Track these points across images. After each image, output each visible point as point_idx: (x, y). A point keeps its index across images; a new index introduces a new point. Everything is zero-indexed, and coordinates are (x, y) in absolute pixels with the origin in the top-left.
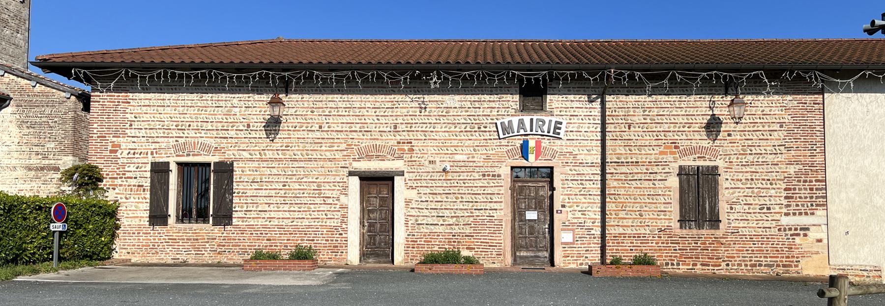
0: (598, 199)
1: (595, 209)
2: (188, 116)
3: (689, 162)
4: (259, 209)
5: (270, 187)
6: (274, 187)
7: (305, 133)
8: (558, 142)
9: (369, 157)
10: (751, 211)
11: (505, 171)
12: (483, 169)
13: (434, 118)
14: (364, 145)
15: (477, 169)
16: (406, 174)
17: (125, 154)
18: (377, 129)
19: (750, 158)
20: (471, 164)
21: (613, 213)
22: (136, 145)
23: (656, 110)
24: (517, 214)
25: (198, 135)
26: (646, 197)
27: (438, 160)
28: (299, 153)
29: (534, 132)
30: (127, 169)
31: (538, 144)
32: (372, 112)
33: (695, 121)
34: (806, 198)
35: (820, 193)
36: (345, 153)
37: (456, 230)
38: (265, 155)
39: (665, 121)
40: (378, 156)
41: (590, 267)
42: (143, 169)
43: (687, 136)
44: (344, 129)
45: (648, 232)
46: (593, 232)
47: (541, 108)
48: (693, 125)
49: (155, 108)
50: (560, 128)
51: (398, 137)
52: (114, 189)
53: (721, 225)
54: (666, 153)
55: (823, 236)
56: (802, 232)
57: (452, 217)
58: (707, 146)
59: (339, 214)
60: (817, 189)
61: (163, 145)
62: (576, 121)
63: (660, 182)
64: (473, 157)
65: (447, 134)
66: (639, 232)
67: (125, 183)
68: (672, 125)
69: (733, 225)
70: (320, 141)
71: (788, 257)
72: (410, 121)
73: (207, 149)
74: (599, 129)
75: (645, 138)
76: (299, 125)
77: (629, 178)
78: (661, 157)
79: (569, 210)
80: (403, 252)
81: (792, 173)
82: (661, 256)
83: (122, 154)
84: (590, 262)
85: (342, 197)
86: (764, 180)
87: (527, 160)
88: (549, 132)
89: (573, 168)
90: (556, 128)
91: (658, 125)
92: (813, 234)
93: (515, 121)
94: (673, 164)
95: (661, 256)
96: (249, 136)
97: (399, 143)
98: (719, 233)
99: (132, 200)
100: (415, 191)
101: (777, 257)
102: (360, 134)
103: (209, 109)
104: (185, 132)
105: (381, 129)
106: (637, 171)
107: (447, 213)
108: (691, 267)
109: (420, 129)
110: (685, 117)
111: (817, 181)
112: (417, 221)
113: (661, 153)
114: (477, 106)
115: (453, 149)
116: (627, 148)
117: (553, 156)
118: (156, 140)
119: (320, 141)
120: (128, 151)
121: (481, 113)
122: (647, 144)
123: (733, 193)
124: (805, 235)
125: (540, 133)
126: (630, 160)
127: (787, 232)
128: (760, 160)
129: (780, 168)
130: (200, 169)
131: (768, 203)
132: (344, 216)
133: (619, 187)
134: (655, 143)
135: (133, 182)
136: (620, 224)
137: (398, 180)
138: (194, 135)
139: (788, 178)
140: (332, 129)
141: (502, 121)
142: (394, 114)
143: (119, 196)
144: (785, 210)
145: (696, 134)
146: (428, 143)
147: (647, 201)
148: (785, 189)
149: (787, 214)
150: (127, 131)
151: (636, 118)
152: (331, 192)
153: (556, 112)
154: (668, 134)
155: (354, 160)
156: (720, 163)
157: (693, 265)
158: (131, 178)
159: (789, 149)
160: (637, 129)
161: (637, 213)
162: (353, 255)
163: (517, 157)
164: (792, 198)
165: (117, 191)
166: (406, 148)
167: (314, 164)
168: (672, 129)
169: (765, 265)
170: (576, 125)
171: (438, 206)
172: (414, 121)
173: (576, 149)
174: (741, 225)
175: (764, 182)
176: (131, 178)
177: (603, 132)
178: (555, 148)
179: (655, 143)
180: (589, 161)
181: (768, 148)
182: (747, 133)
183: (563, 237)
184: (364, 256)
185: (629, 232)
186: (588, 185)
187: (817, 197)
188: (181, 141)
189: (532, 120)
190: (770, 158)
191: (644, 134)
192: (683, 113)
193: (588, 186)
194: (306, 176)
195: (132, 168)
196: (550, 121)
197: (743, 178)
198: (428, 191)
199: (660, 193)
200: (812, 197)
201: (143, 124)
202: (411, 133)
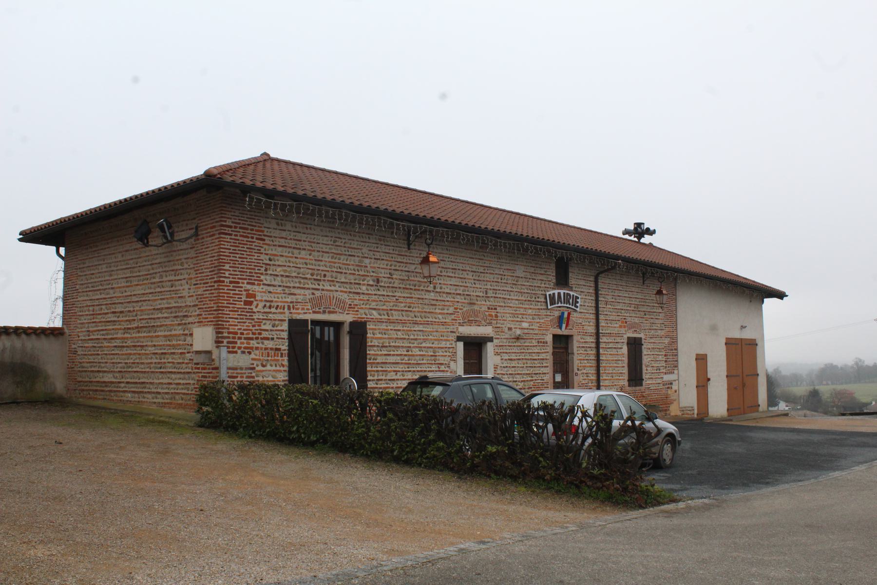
0: (594, 363)
4: (388, 378)
5: (396, 353)
6: (399, 353)
9: (470, 323)
11: (549, 338)
20: (531, 332)
22: (272, 295)
25: (333, 288)
30: (263, 327)
36: (453, 317)
38: (392, 315)
42: (279, 328)
49: (291, 250)
52: (250, 353)
67: (260, 345)
70: (434, 302)
73: (342, 306)
83: (258, 307)
85: (452, 363)
87: (561, 328)
92: (675, 387)
98: (642, 388)
99: (268, 367)
100: (499, 357)
103: (342, 257)
104: (321, 283)
118: (293, 291)
119: (434, 302)
120: (263, 303)
130: (326, 329)
135: (270, 344)
137: (490, 347)
138: (329, 288)
140: (443, 290)
143: (255, 363)
150: (262, 277)
155: (461, 325)
158: (267, 339)
165: (252, 356)
176: (267, 339)
188: (318, 294)
194: (425, 340)
195: (268, 327)
201: (279, 269)
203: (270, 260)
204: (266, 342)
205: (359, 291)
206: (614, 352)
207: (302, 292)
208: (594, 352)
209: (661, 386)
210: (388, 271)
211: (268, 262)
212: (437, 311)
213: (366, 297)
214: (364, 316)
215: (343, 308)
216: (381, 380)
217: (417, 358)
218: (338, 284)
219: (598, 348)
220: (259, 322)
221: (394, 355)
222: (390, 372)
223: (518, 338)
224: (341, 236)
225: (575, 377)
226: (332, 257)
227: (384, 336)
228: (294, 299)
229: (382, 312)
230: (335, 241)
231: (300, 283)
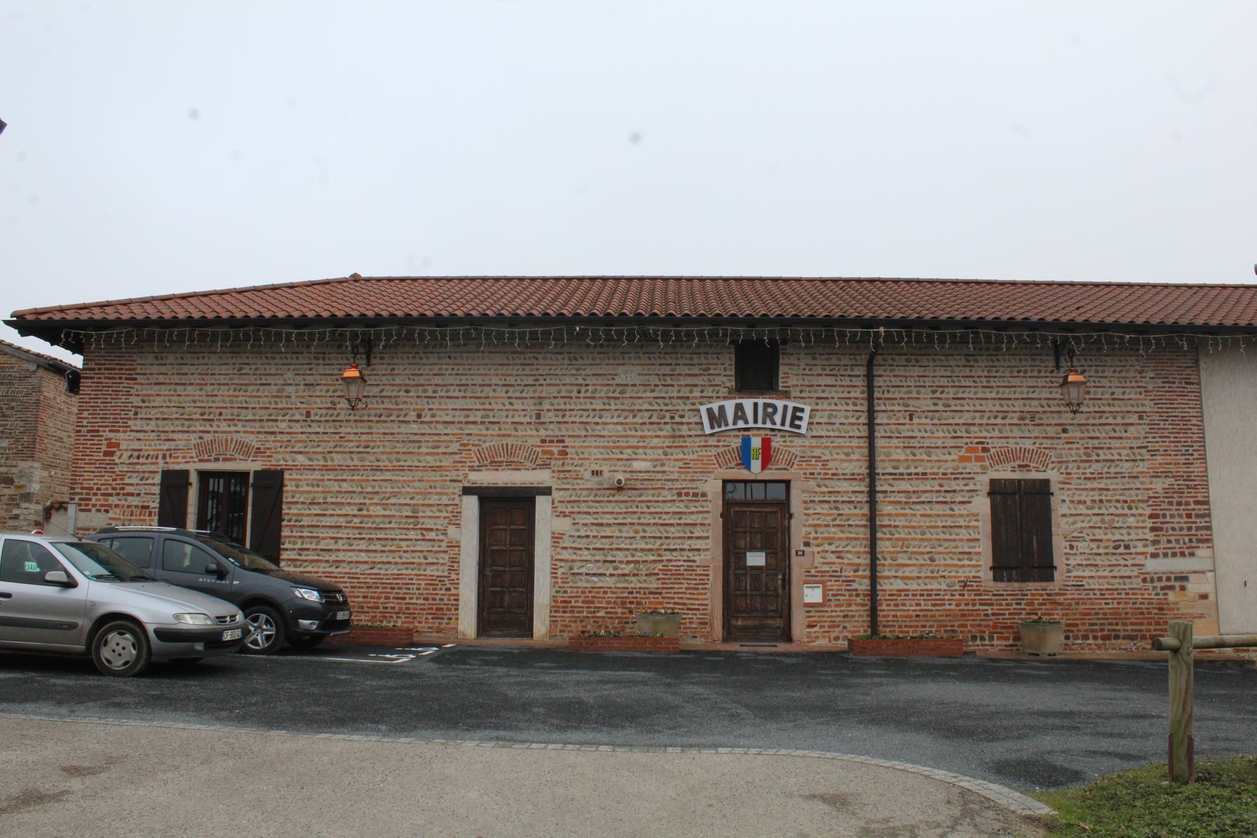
0: (864, 533)
1: (858, 549)
2: (216, 399)
3: (1005, 473)
5: (338, 512)
7: (395, 425)
8: (798, 442)
9: (496, 465)
10: (1101, 551)
11: (713, 487)
12: (677, 485)
13: (600, 401)
14: (487, 445)
15: (669, 485)
16: (554, 492)
17: (125, 458)
18: (510, 420)
19: (1096, 467)
20: (659, 476)
21: (888, 556)
22: (142, 443)
23: (952, 390)
25: (233, 429)
26: (939, 530)
27: (605, 469)
28: (384, 457)
29: (760, 425)
30: (127, 481)
31: (766, 443)
32: (501, 392)
33: (1012, 409)
34: (1181, 529)
35: (1201, 522)
36: (457, 458)
37: (635, 583)
38: (332, 459)
39: (966, 408)
40: (509, 463)
41: (851, 642)
42: (150, 481)
43: (1000, 431)
44: (456, 420)
45: (944, 587)
46: (855, 586)
48: (1010, 415)
49: (172, 387)
50: (800, 419)
51: (543, 433)
52: (107, 511)
53: (1057, 574)
54: (968, 459)
55: (1207, 588)
56: (1177, 584)
57: (628, 562)
58: (1031, 447)
59: (446, 556)
60: (1197, 516)
61: (181, 444)
62: (826, 407)
63: (962, 507)
64: (663, 465)
65: (619, 427)
66: (929, 587)
67: (123, 502)
68: (978, 415)
69: (1074, 574)
71: (1159, 624)
72: (563, 407)
73: (245, 450)
74: (864, 419)
75: (936, 435)
76: (385, 412)
78: (961, 465)
79: (817, 549)
80: (547, 623)
81: (1160, 490)
82: (965, 626)
84: (849, 635)
85: (452, 530)
86: (1118, 501)
88: (783, 424)
89: (822, 482)
90: (794, 418)
91: (957, 415)
92: (1194, 587)
93: (730, 406)
94: (978, 478)
95: (965, 626)
96: (309, 430)
97: (543, 441)
98: (1053, 587)
100: (568, 521)
101: (1142, 624)
102: (482, 427)
103: (251, 388)
104: (214, 424)
105: (516, 419)
106: (924, 488)
107: (620, 556)
108: (1011, 642)
109: (578, 420)
110: (997, 402)
111: (1196, 503)
112: (571, 568)
113: (962, 459)
114: (669, 382)
115: (629, 451)
116: (908, 451)
117: (790, 463)
118: (171, 436)
120: (129, 453)
121: (675, 394)
122: (940, 443)
123: (1074, 523)
124: (1183, 588)
125: (769, 425)
126: (912, 470)
127: (1156, 584)
128: (1112, 470)
129: (1142, 483)
131: (1126, 537)
132: (455, 560)
133: (897, 515)
134: (951, 443)
136: (900, 574)
137: (542, 503)
138: (227, 429)
139: (1153, 500)
141: (709, 406)
142: (537, 395)
144: (1151, 550)
145: (1015, 429)
146: (590, 442)
147: (942, 536)
148: (1151, 516)
149: (1154, 556)
151: (922, 402)
152: (432, 521)
153: (795, 393)
154: (972, 428)
155: (472, 469)
156: (1052, 475)
157: (1015, 639)
158: (132, 495)
159: (1153, 453)
160: (923, 421)
161: (926, 556)
162: (467, 622)
163: (733, 464)
164: (1161, 529)
165: (111, 514)
166: (555, 450)
167: (408, 476)
168: (977, 421)
169: (1125, 637)
170: (826, 413)
171: (605, 544)
172: (568, 407)
173: (827, 452)
174: (1087, 573)
175: (1119, 505)
176: (132, 495)
177: (871, 425)
178: (793, 450)
179: (951, 443)
180: (848, 471)
181: (1124, 452)
182: (1090, 428)
184: (484, 626)
185: (915, 587)
186: (846, 509)
187: (1198, 529)
188: (207, 437)
189: (756, 405)
190: (1126, 467)
191: (934, 429)
192: (993, 395)
193: (847, 511)
194: (394, 495)
196: (785, 407)
197: (1088, 499)
198: (589, 519)
199: (962, 523)
200: (1190, 529)
202: (562, 426)
203: (143, 401)
204: (130, 498)
205: (275, 429)
206: (939, 509)
207: (185, 436)
208: (866, 510)
209: (1137, 583)
210: (329, 400)
211: (141, 404)
212: (423, 450)
213: (285, 438)
214: (282, 462)
215: (247, 454)
216: (307, 549)
217: (378, 520)
218: (240, 424)
219: (872, 502)
220: (122, 475)
221: (332, 515)
222: (324, 539)
223: (620, 489)
224: (251, 361)
225: (795, 560)
226: (235, 390)
227: (316, 489)
228: (172, 445)
229: (314, 456)
230: (241, 369)
231: (183, 425)
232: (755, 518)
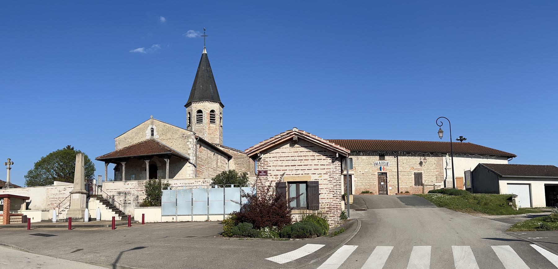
3: (416, 171)
11: (376, 173)
24: (379, 183)
47: (384, 159)
77: (403, 175)
183: (390, 188)
232: (383, 176)
